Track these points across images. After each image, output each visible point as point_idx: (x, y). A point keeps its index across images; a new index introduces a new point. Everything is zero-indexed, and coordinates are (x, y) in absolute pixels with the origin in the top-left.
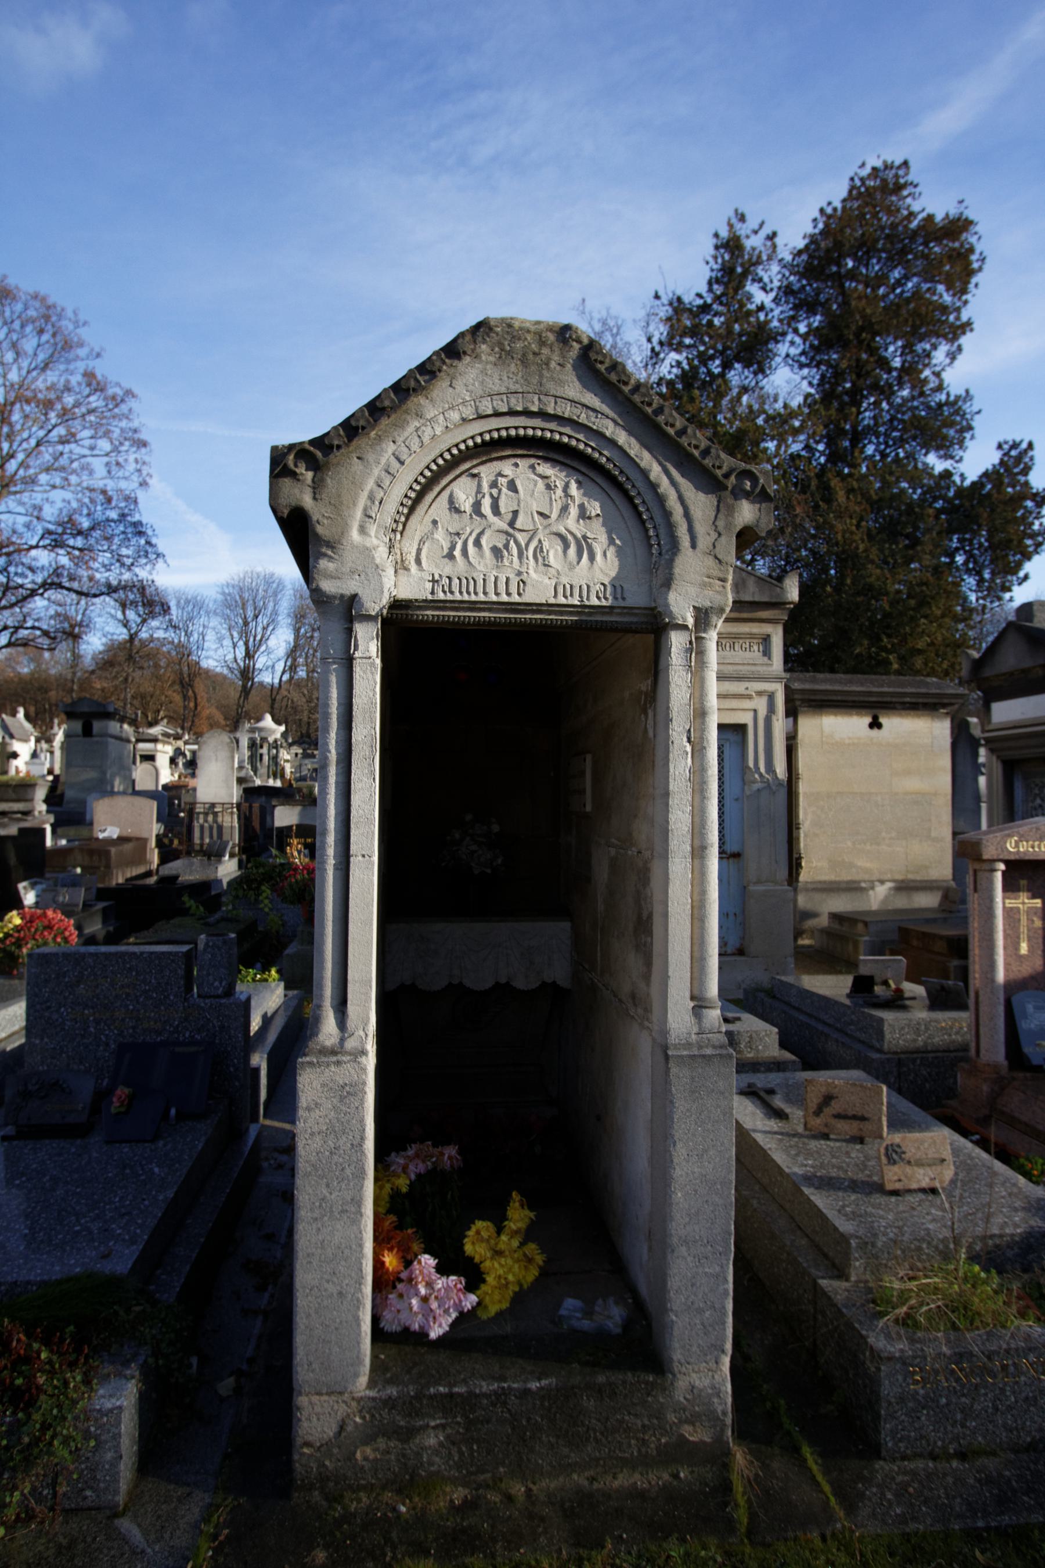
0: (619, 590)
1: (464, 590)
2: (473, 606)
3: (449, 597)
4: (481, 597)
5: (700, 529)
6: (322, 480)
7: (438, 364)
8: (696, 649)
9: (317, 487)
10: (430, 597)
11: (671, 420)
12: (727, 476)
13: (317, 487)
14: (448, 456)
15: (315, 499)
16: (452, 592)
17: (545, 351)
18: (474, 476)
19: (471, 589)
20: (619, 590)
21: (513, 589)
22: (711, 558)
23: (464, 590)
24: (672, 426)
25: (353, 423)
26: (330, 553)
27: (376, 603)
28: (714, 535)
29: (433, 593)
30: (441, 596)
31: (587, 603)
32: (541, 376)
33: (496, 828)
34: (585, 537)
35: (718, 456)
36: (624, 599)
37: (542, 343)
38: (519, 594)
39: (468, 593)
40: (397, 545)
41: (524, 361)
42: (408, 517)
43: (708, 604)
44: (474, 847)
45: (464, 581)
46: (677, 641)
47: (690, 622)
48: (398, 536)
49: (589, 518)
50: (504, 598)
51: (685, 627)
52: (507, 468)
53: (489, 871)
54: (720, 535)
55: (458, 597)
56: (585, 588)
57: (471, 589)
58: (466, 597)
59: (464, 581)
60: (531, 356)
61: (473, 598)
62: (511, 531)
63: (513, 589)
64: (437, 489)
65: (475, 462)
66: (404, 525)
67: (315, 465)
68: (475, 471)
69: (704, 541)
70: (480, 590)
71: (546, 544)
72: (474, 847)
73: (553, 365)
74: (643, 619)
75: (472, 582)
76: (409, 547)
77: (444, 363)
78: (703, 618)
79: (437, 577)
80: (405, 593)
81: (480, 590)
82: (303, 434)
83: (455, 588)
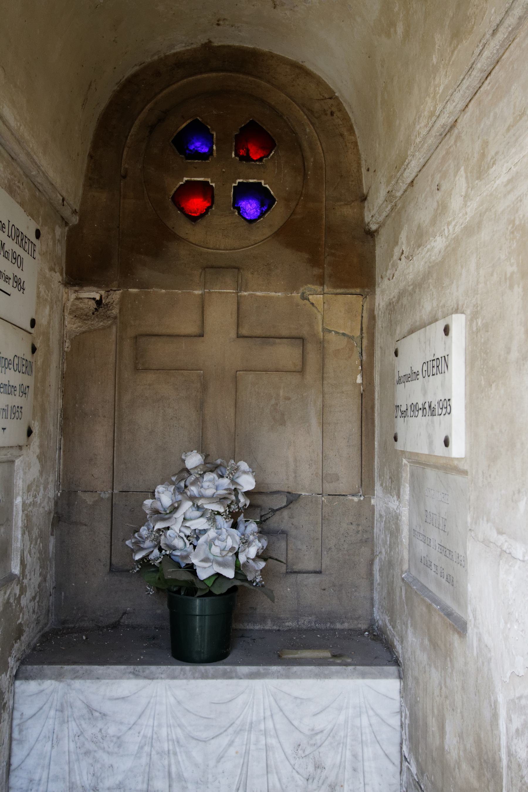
33: (247, 483)
44: (201, 524)
53: (230, 573)
72: (201, 524)
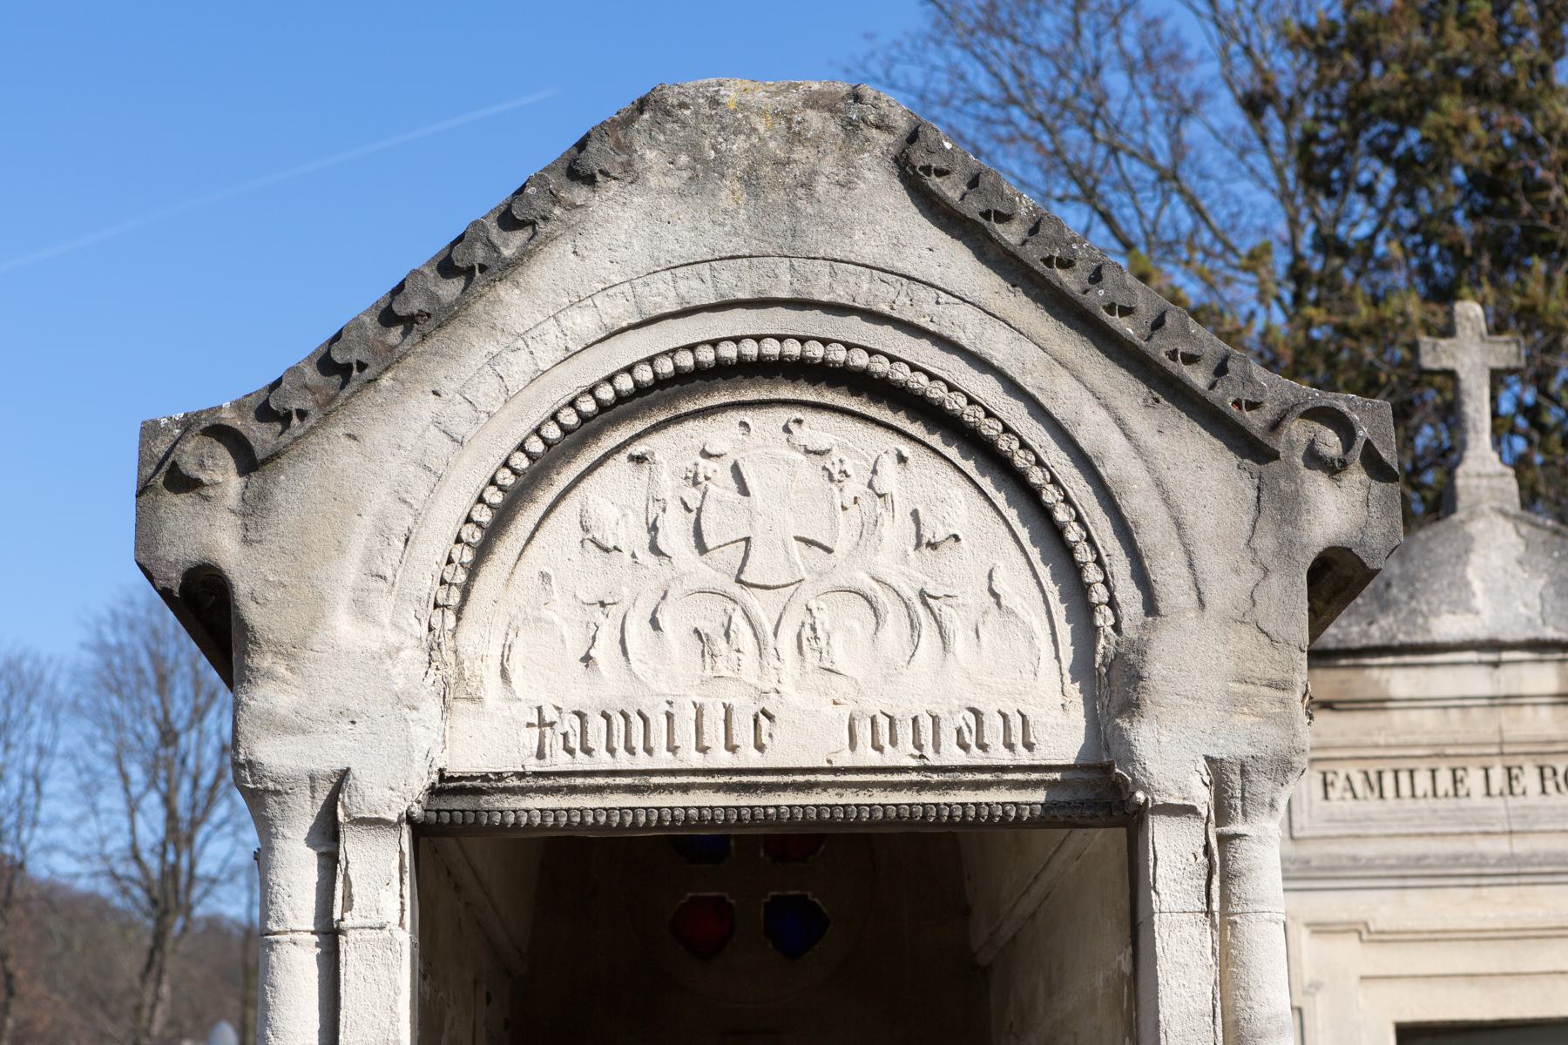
0: (1016, 722)
1: (619, 743)
2: (640, 783)
3: (582, 762)
4: (663, 759)
5: (1213, 564)
6: (263, 496)
7: (540, 204)
8: (1221, 866)
9: (253, 510)
10: (533, 765)
11: (1121, 300)
12: (1275, 426)
13: (253, 510)
14: (536, 446)
15: (246, 541)
16: (588, 751)
17: (800, 153)
18: (639, 459)
19: (637, 741)
20: (1016, 722)
21: (743, 733)
22: (1248, 634)
23: (619, 743)
24: (1126, 311)
25: (338, 357)
26: (281, 669)
27: (392, 786)
28: (1251, 574)
29: (540, 755)
30: (561, 761)
31: (934, 761)
32: (794, 212)
34: (923, 595)
35: (1248, 379)
36: (1029, 746)
37: (795, 137)
38: (760, 747)
39: (631, 750)
40: (446, 643)
41: (751, 181)
42: (473, 571)
43: (1243, 750)
45: (618, 722)
46: (1173, 851)
47: (1202, 797)
48: (451, 618)
49: (933, 546)
50: (722, 759)
51: (1188, 811)
52: (721, 433)
54: (1266, 571)
55: (602, 761)
56: (926, 725)
57: (637, 741)
58: (623, 761)
59: (618, 722)
60: (767, 170)
61: (642, 761)
62: (736, 590)
63: (743, 733)
64: (546, 497)
65: (639, 426)
66: (466, 592)
67: (248, 461)
68: (638, 449)
69: (1226, 587)
70: (659, 739)
71: (823, 619)
73: (821, 185)
74: (1083, 795)
75: (637, 723)
76: (478, 641)
77: (556, 200)
78: (1228, 788)
79: (550, 715)
80: (467, 760)
81: (659, 739)
82: (225, 389)
83: (597, 739)
